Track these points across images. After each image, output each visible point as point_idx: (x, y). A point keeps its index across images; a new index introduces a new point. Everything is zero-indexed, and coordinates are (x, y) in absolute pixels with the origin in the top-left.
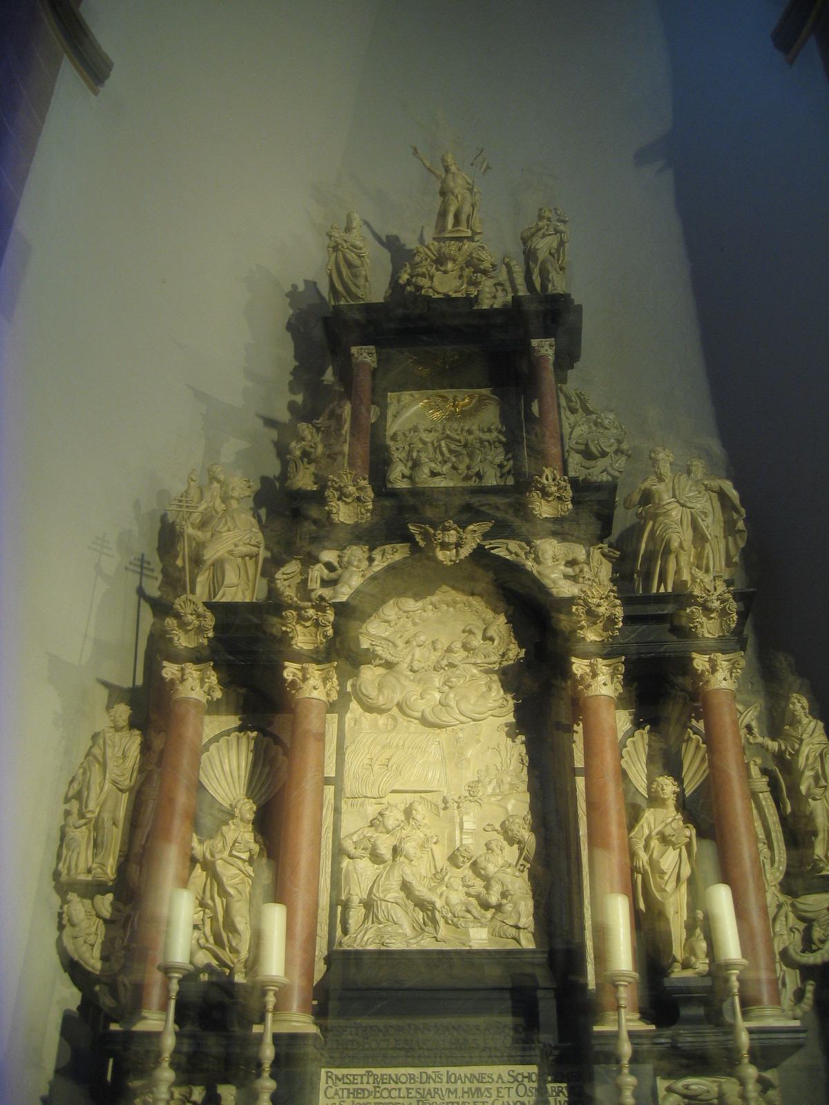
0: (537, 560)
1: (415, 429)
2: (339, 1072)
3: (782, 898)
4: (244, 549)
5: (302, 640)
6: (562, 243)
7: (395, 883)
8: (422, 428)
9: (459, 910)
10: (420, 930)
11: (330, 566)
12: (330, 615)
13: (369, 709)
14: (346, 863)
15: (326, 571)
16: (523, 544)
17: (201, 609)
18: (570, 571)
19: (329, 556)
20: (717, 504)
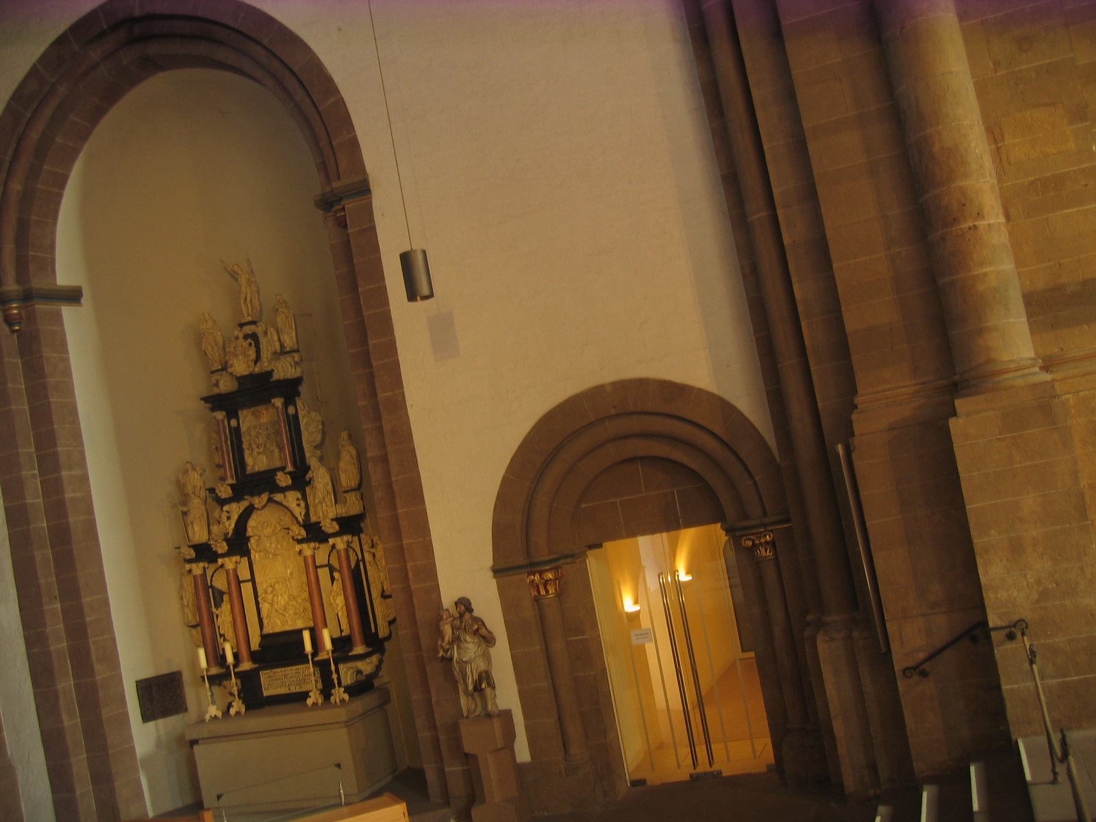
0: (288, 501)
1: (249, 428)
2: (264, 672)
3: (382, 599)
4: (197, 516)
5: (220, 551)
6: (287, 317)
7: (274, 611)
8: (252, 429)
9: (293, 615)
10: (283, 625)
11: (228, 512)
12: (225, 544)
13: (256, 552)
14: (260, 605)
15: (227, 514)
16: (282, 494)
17: (187, 549)
18: (298, 502)
19: (226, 508)
20: (348, 457)
